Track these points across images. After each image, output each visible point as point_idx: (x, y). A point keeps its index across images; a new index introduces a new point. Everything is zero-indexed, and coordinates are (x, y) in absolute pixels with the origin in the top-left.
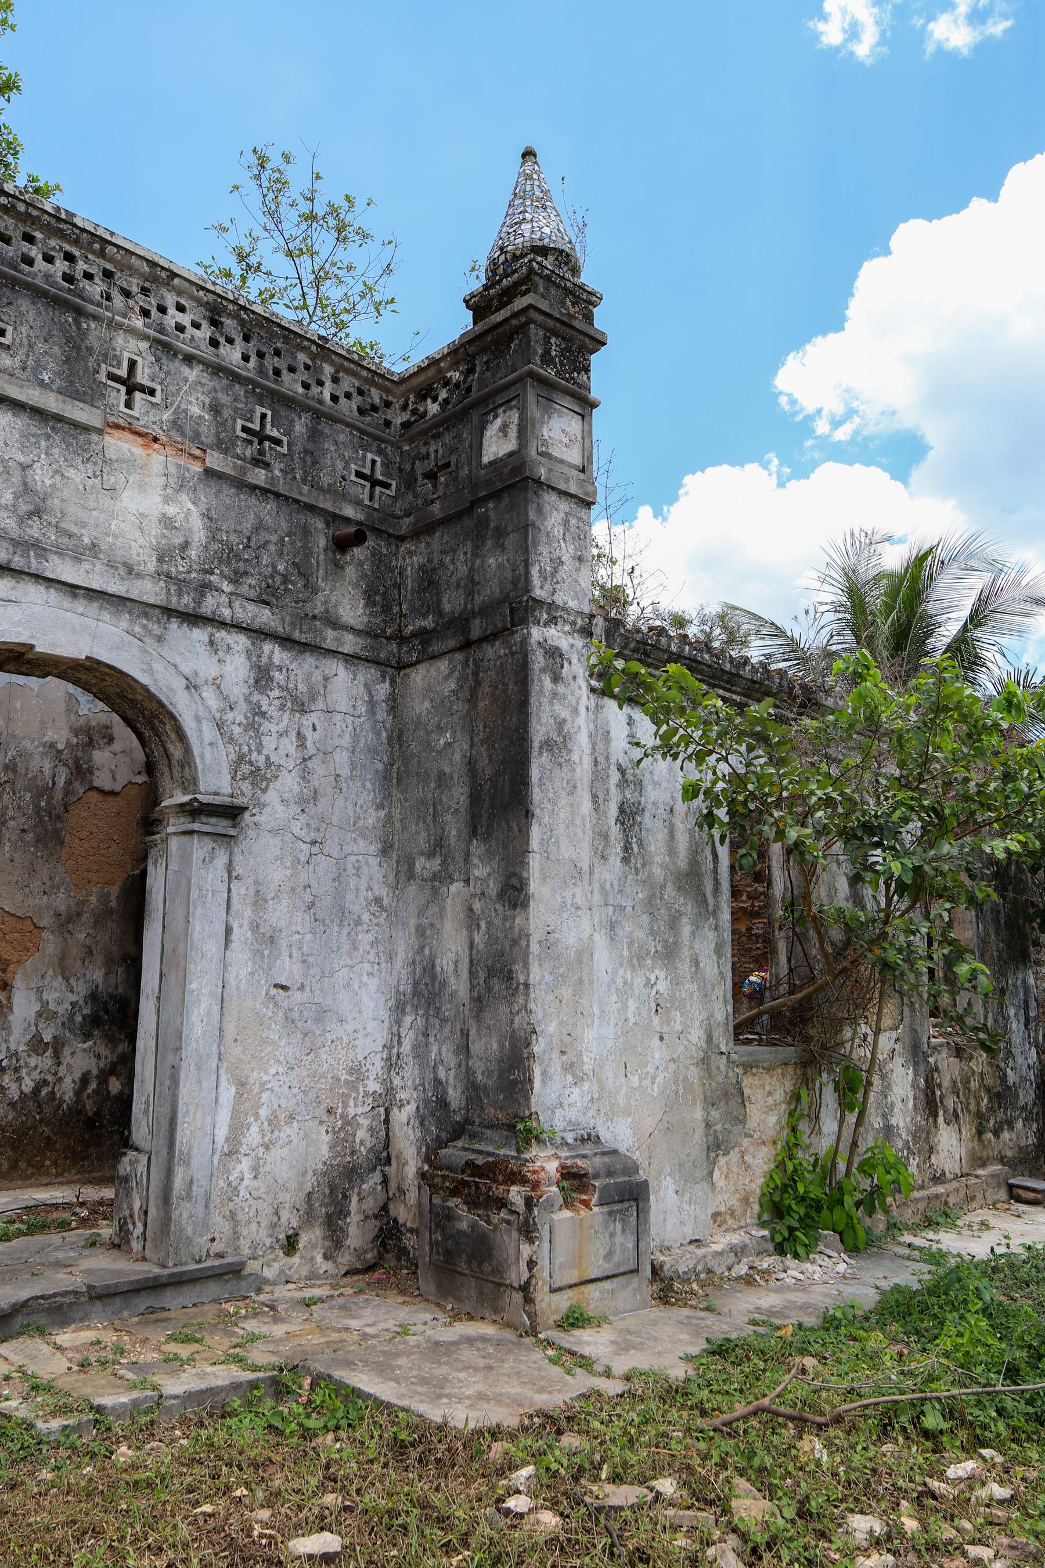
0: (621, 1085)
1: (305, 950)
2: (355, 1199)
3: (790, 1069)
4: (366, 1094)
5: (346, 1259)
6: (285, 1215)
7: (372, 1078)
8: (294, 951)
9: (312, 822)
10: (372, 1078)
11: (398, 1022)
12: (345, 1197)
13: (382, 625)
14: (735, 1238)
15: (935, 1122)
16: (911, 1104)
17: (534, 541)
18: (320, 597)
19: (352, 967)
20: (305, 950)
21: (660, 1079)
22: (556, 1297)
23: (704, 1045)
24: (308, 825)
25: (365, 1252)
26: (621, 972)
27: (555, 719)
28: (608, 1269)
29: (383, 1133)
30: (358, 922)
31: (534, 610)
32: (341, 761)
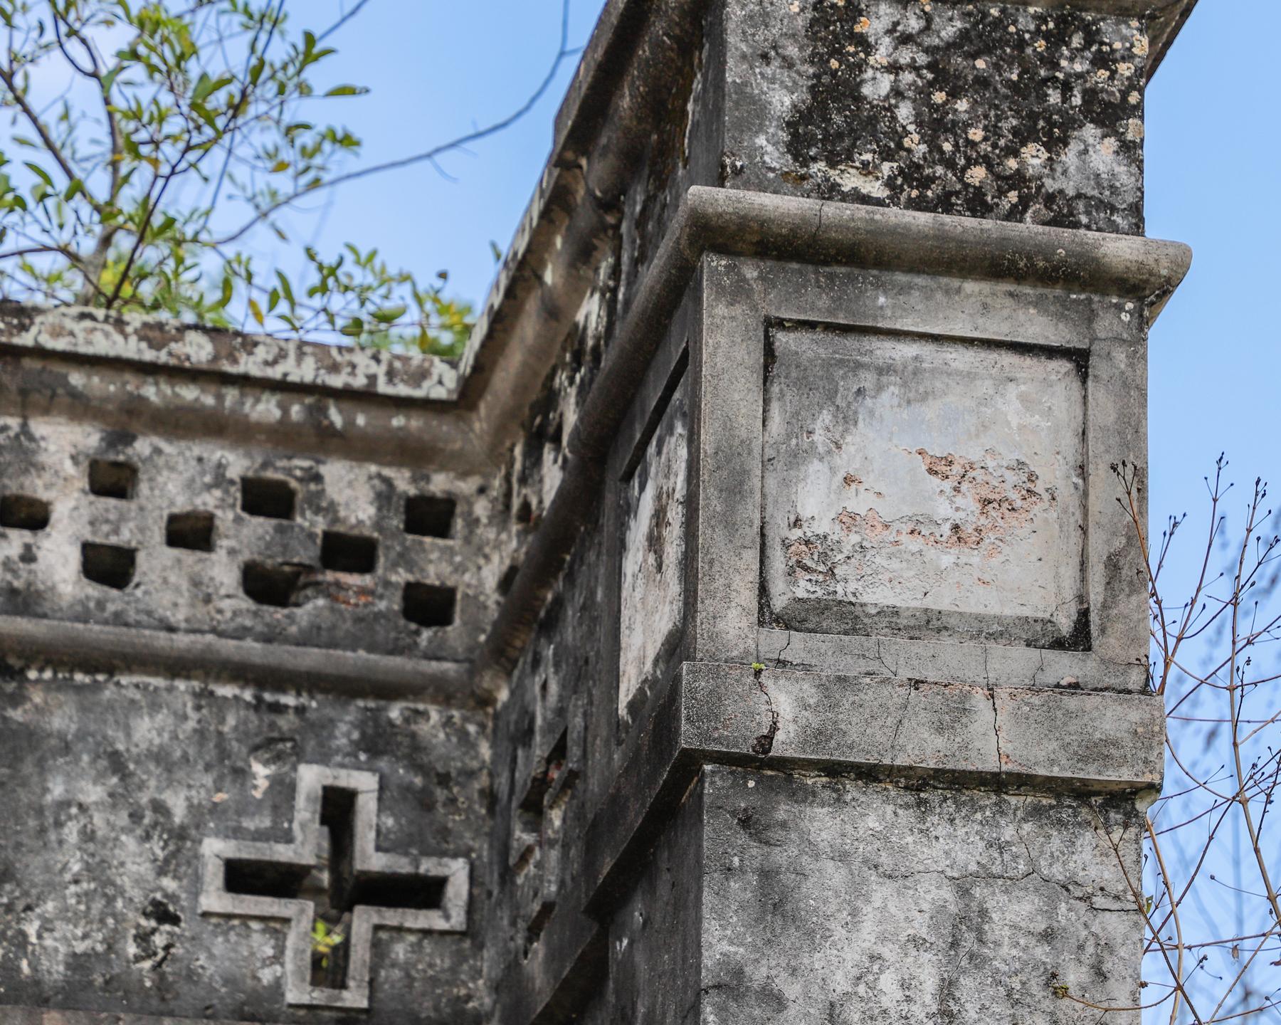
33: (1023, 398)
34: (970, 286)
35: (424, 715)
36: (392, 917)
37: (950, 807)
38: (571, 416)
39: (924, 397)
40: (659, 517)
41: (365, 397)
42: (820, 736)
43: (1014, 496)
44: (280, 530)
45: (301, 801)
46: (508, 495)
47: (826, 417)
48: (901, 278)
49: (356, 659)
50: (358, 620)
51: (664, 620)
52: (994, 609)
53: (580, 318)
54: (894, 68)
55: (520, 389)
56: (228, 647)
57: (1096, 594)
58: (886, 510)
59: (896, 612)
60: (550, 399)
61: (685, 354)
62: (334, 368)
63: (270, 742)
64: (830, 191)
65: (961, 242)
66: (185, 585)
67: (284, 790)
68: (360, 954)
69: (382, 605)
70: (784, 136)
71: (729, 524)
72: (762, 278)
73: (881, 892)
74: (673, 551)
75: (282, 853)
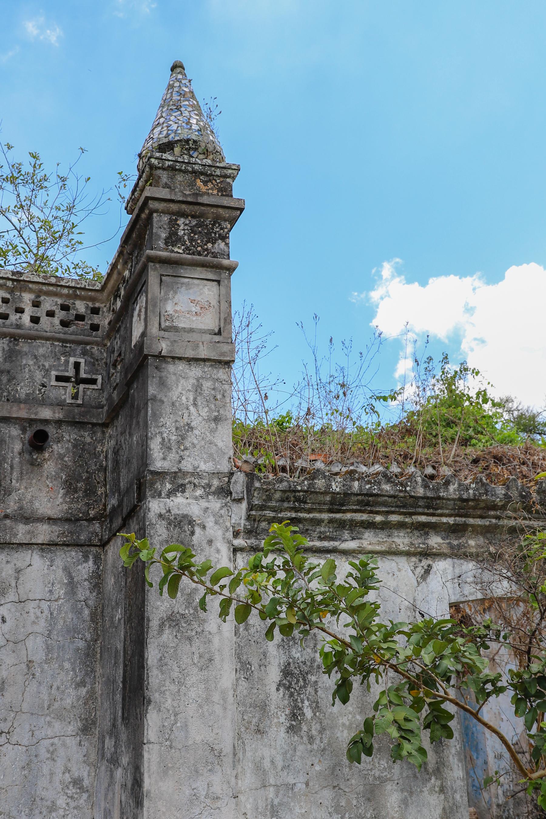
17: (154, 414)
31: (152, 484)
33: (208, 289)
34: (198, 269)
35: (94, 348)
36: (87, 386)
37: (195, 365)
38: (123, 293)
39: (190, 289)
40: (140, 311)
41: (84, 289)
42: (171, 351)
43: (207, 307)
44: (67, 313)
45: (70, 364)
46: (110, 307)
47: (172, 292)
48: (186, 267)
49: (81, 338)
50: (82, 330)
51: (141, 330)
52: (203, 328)
53: (125, 274)
54: (184, 230)
55: (113, 287)
56: (57, 335)
57: (222, 326)
58: (183, 310)
59: (185, 328)
60: (118, 289)
61: (145, 281)
62: (78, 284)
63: (65, 353)
64: (172, 251)
65: (196, 261)
66: (49, 323)
67: (67, 362)
68: (81, 393)
69: (86, 327)
70: (164, 242)
71: (153, 312)
72: (160, 267)
73: (182, 381)
74: (143, 317)
75: (66, 374)
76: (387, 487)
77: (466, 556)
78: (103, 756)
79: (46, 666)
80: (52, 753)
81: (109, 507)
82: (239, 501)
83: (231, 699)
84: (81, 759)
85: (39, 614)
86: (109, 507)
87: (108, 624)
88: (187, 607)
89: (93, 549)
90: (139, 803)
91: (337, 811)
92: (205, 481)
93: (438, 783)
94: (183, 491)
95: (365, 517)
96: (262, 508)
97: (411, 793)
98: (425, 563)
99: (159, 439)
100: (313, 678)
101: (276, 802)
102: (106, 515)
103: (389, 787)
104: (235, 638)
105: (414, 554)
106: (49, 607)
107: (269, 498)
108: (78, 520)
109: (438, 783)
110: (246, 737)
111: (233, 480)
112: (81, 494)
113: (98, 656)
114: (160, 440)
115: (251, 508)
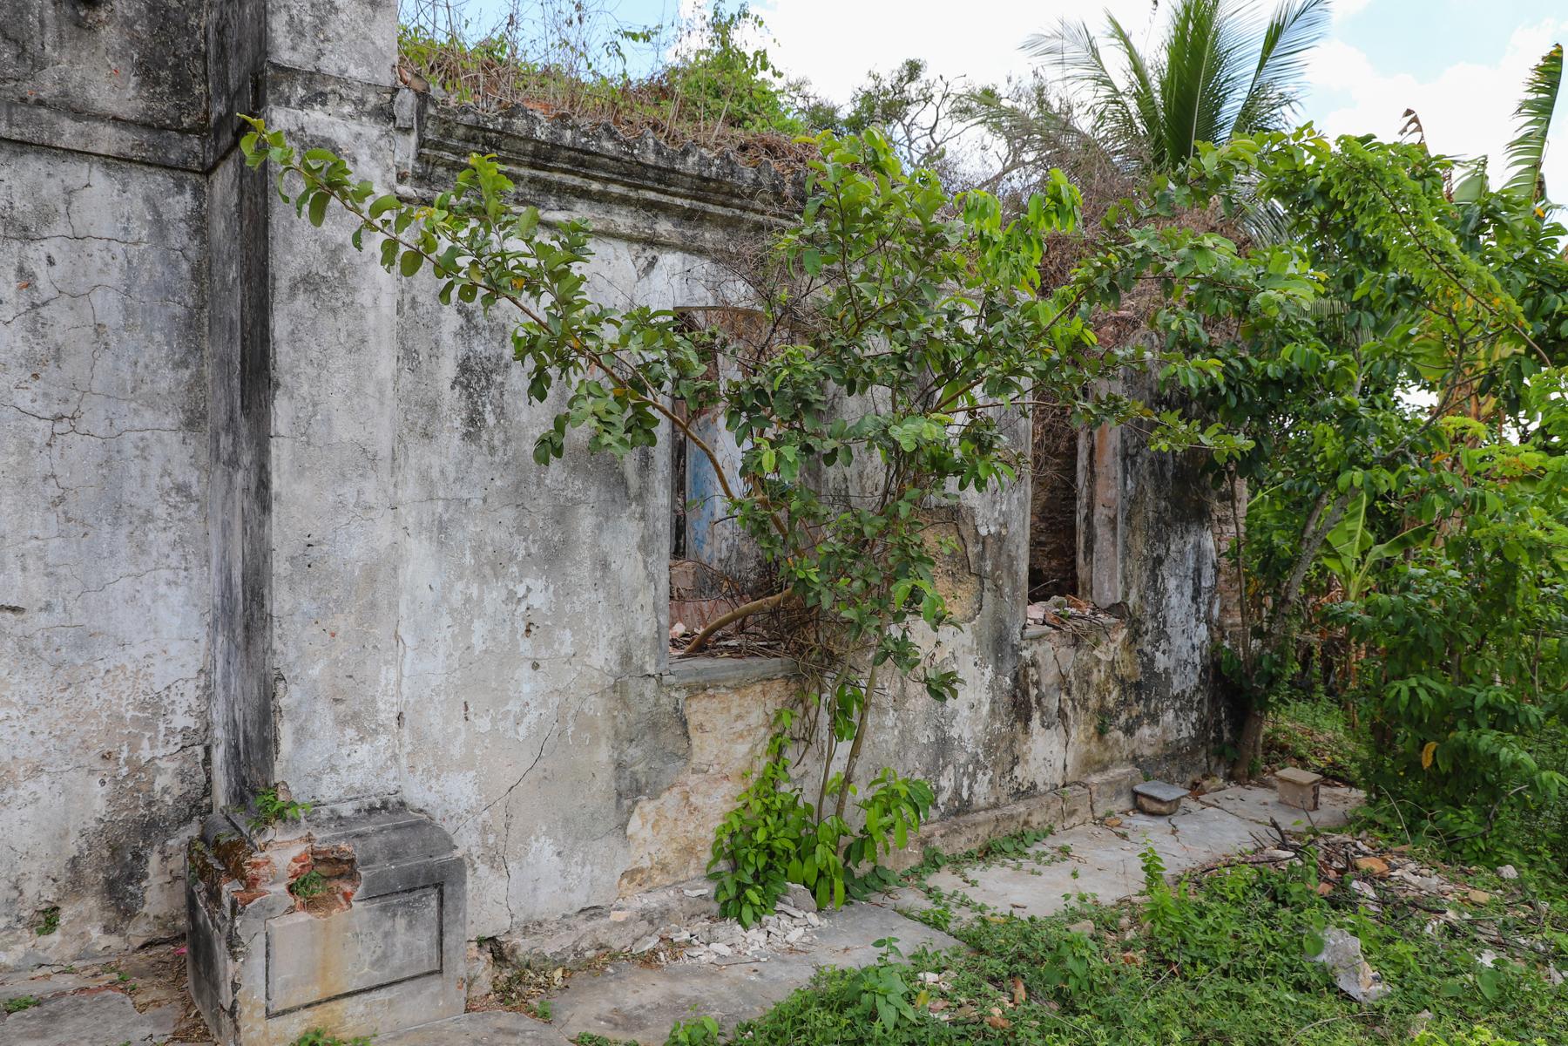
0: (457, 731)
1: (50, 559)
2: (154, 860)
3: (778, 686)
4: (170, 732)
5: (139, 931)
6: (30, 889)
7: (180, 711)
8: (30, 562)
9: (54, 391)
10: (180, 711)
11: (214, 641)
12: (137, 856)
13: (173, 112)
14: (653, 901)
15: (1026, 726)
16: (985, 709)
18: (50, 73)
19: (137, 576)
20: (50, 559)
21: (531, 717)
22: (276, 1023)
23: (616, 669)
24: (45, 395)
25: (175, 919)
26: (460, 586)
27: (323, 245)
28: (379, 977)
29: (201, 777)
30: (148, 518)
31: (276, 84)
32: (107, 306)
76: (608, 145)
77: (701, 252)
78: (218, 458)
79: (125, 335)
80: (143, 450)
81: (213, 116)
82: (406, 131)
83: (389, 393)
84: (187, 460)
85: (109, 259)
86: (213, 116)
87: (218, 286)
88: (329, 268)
89: (190, 176)
90: (265, 508)
91: (519, 532)
92: (356, 95)
93: (639, 509)
94: (324, 104)
95: (577, 181)
96: (438, 146)
97: (607, 518)
98: (650, 253)
99: (285, 17)
100: (499, 379)
101: (446, 517)
102: (208, 130)
103: (582, 510)
104: (397, 318)
105: (637, 241)
106: (125, 252)
107: (448, 134)
108: (164, 128)
109: (639, 509)
110: (411, 441)
111: (397, 100)
112: (166, 88)
113: (206, 329)
114: (287, 18)
115: (422, 143)
